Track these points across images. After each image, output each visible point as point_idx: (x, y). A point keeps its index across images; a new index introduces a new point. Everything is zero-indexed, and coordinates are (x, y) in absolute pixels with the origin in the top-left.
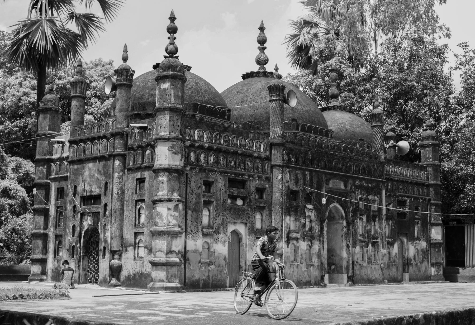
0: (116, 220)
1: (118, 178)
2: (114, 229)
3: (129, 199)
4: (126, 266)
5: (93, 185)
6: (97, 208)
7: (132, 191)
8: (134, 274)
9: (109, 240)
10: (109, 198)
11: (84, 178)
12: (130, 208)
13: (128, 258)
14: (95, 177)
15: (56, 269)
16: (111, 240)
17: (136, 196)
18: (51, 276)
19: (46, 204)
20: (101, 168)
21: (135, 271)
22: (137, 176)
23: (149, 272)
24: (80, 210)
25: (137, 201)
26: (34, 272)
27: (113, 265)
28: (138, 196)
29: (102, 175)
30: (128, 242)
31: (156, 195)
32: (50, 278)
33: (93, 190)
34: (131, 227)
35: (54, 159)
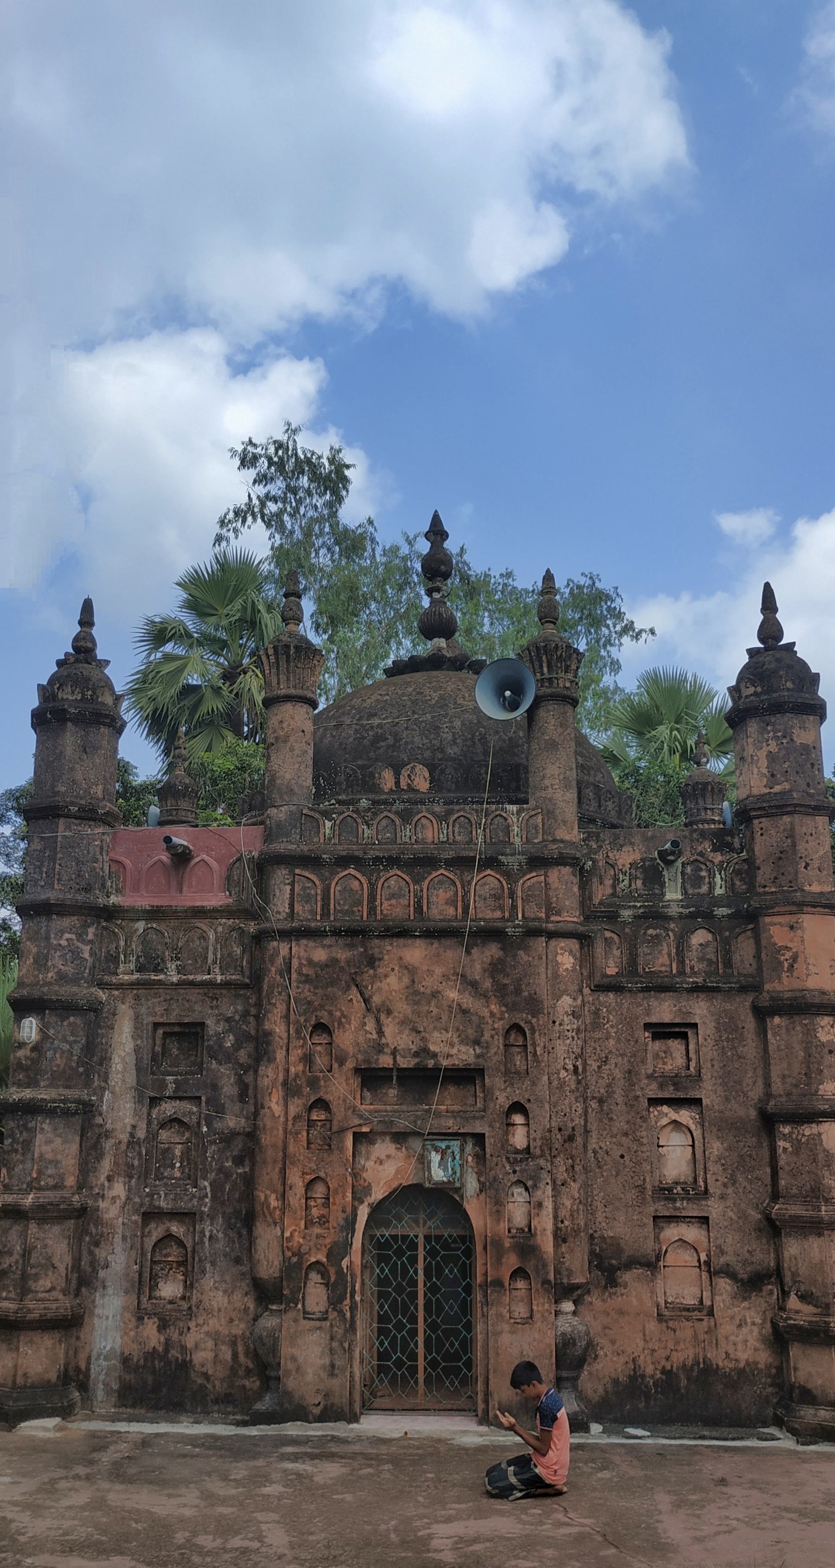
0: (577, 1168)
1: (573, 1014)
2: (568, 1203)
3: (610, 1094)
4: (613, 1342)
5: (435, 1028)
6: (467, 1119)
7: (627, 1067)
8: (664, 1371)
9: (547, 1244)
10: (534, 1084)
11: (376, 1000)
12: (620, 1124)
13: (621, 1313)
14: (445, 1003)
15: (152, 1354)
16: (556, 1246)
17: (654, 1086)
18: (115, 1386)
19: (88, 1084)
20: (476, 972)
21: (667, 1358)
22: (648, 1012)
23: (748, 1363)
24: (357, 1121)
25: (655, 1102)
26: (25, 1375)
27: (574, 1344)
28: (661, 1086)
29: (485, 996)
30: (619, 1250)
31: (817, 1091)
32: (108, 1392)
33: (432, 1048)
34: (632, 1194)
35: (132, 910)
